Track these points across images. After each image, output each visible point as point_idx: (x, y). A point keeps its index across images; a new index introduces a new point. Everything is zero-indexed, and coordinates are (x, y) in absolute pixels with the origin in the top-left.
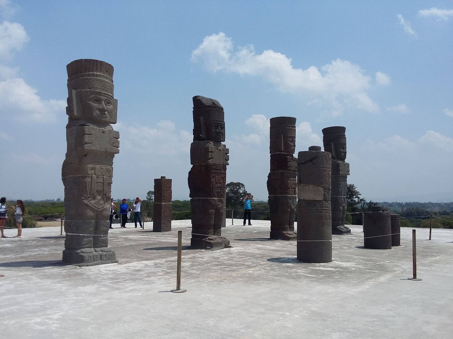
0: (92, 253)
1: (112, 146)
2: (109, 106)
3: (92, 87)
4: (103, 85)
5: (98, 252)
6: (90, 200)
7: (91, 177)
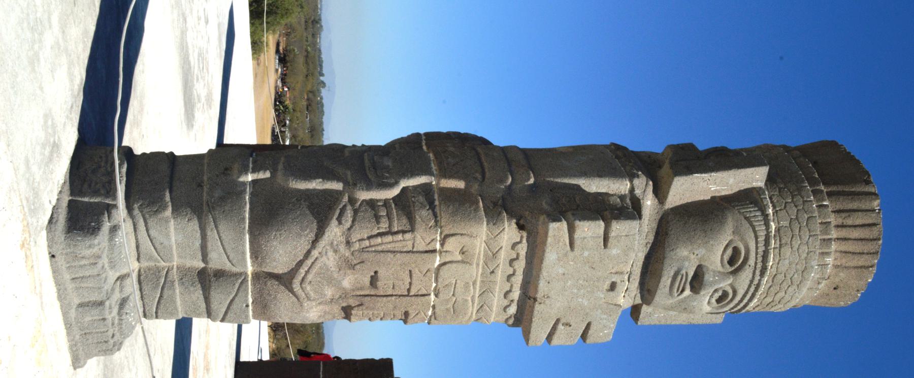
0: (113, 265)
1: (558, 321)
2: (709, 302)
3: (783, 242)
4: (789, 277)
5: (117, 290)
6: (336, 251)
7: (434, 251)
